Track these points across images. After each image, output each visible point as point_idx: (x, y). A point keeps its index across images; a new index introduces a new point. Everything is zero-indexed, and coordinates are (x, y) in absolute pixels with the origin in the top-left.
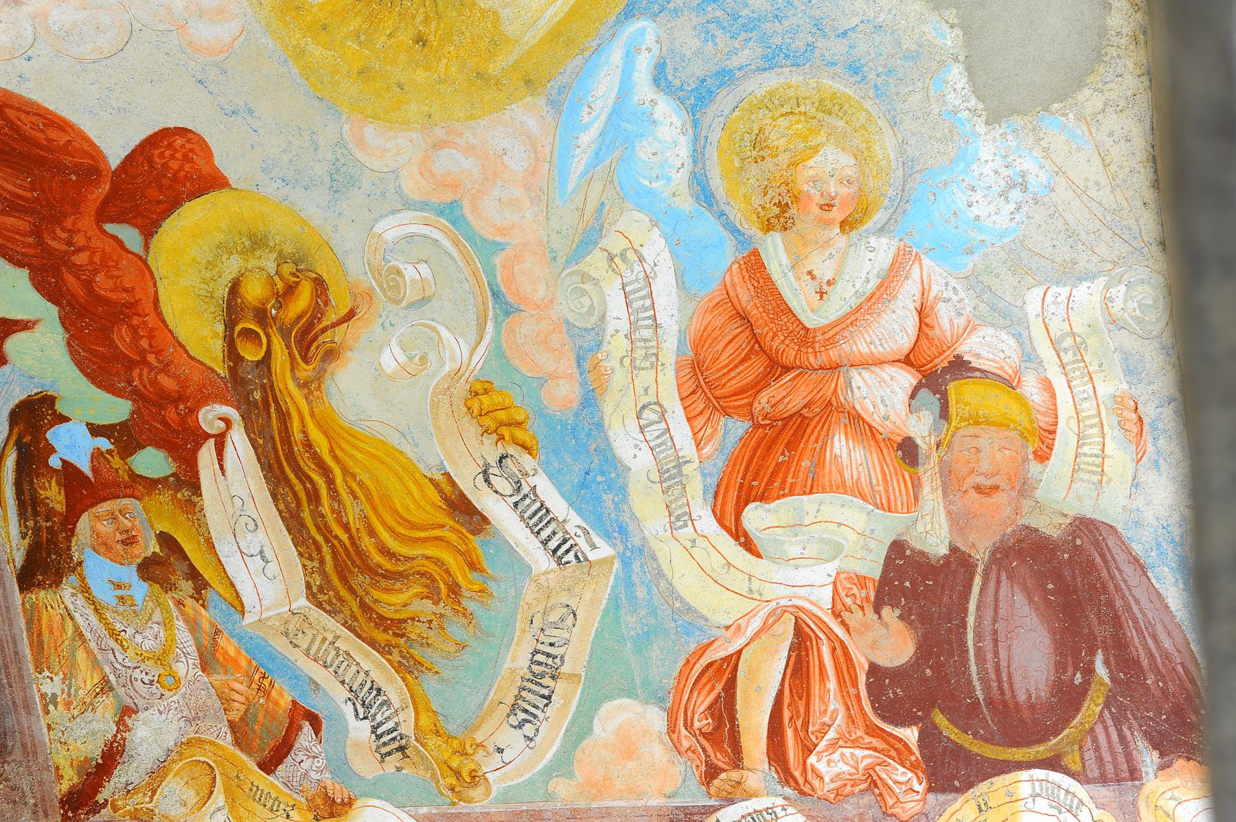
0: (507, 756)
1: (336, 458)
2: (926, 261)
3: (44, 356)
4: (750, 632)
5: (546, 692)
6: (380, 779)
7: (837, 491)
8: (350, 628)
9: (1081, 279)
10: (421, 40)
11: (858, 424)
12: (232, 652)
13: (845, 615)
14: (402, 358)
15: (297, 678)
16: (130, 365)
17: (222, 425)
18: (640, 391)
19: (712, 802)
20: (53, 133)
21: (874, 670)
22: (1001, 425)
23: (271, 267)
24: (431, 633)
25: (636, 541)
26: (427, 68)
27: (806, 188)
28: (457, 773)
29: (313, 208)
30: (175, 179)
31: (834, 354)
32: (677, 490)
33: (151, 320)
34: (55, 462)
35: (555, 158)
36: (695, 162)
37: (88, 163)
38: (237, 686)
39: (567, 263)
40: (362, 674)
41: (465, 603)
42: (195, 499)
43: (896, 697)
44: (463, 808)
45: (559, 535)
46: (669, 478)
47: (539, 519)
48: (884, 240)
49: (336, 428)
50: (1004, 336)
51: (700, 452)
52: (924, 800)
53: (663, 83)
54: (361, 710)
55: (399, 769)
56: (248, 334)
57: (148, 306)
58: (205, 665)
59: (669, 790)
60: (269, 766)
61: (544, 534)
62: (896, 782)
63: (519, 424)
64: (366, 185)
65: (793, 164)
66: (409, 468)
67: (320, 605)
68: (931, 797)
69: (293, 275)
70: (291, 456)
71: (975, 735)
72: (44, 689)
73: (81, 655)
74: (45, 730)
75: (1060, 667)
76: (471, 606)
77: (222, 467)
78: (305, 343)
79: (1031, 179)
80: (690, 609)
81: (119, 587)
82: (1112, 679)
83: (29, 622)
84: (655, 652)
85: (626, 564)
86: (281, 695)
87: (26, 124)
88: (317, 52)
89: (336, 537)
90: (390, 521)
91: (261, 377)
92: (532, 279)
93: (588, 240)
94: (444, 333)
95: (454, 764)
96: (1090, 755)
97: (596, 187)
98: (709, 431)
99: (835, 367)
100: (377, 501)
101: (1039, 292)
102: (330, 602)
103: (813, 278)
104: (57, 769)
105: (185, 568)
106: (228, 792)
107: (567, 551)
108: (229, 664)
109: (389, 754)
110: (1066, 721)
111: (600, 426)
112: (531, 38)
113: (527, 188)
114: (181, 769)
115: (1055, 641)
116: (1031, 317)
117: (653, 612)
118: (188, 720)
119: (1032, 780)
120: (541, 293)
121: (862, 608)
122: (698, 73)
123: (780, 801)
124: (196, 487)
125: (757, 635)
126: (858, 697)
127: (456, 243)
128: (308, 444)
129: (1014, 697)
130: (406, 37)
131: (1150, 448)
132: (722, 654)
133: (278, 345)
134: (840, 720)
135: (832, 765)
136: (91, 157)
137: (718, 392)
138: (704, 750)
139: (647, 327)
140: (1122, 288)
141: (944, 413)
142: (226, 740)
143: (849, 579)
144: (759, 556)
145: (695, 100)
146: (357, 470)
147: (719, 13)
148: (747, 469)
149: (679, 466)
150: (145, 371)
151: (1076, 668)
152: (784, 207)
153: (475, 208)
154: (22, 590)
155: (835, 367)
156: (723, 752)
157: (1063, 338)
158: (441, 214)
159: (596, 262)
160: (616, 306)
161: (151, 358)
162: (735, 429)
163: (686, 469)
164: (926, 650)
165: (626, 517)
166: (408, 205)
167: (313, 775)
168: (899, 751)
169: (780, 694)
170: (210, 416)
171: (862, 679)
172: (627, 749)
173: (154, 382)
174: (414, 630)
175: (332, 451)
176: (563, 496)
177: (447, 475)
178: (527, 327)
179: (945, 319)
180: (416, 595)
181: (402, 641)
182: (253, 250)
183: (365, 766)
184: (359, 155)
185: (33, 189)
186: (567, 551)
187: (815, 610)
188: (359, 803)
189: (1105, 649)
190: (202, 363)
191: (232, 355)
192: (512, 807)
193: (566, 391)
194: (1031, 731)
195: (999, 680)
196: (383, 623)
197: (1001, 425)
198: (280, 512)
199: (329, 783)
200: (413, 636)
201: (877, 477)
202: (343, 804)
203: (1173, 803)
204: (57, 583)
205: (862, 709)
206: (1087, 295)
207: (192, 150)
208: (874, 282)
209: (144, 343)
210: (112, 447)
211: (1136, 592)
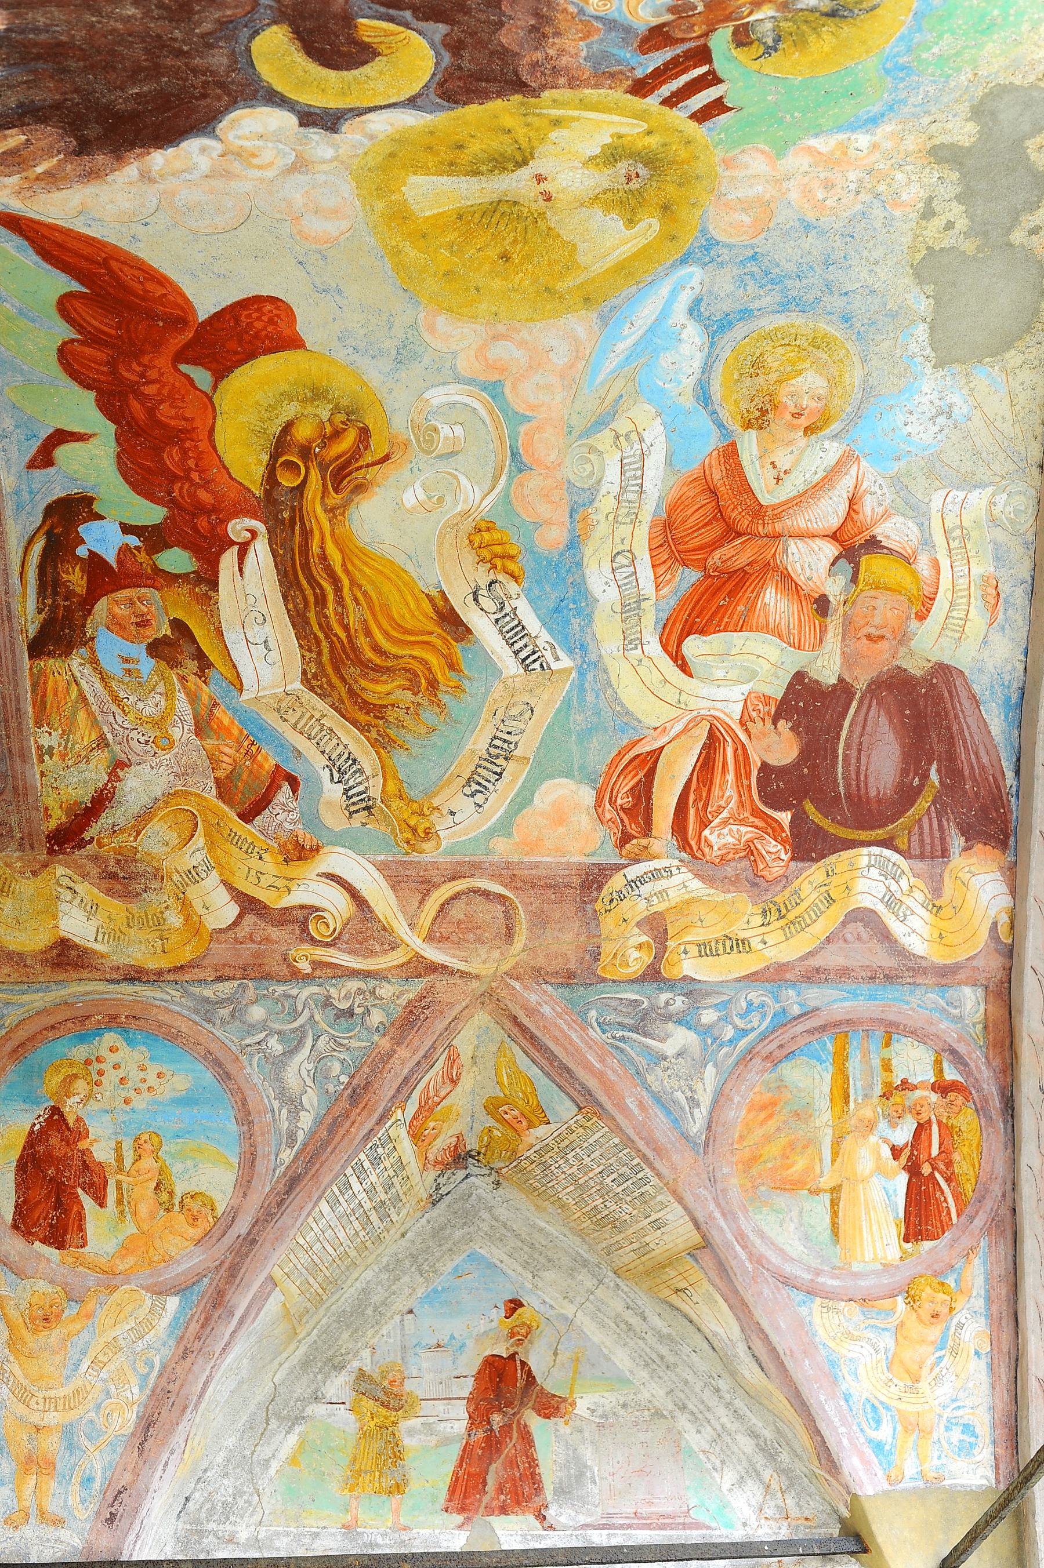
0: (457, 818)
1: (346, 571)
2: (864, 463)
3: (93, 463)
4: (673, 733)
5: (498, 770)
6: (348, 831)
7: (761, 631)
8: (336, 709)
9: (975, 487)
10: (505, 257)
11: (788, 582)
12: (226, 722)
13: (750, 724)
14: (422, 496)
15: (281, 745)
16: (174, 478)
17: (248, 535)
18: (618, 540)
19: (622, 861)
20: (150, 286)
21: (765, 767)
22: (895, 591)
23: (325, 415)
24: (407, 717)
25: (593, 657)
26: (505, 279)
27: (784, 399)
28: (414, 830)
29: (375, 374)
30: (256, 336)
31: (778, 526)
32: (634, 620)
33: (203, 445)
34: (82, 552)
35: (592, 358)
36: (703, 372)
37: (174, 311)
38: (226, 750)
39: (580, 437)
40: (341, 747)
41: (440, 695)
42: (211, 593)
43: (776, 787)
44: (415, 857)
45: (530, 648)
46: (629, 611)
47: (514, 632)
48: (835, 444)
49: (351, 546)
50: (910, 524)
51: (658, 592)
52: (787, 866)
53: (696, 313)
54: (336, 776)
55: (364, 824)
56: (290, 466)
57: (203, 435)
58: (200, 730)
59: (588, 851)
60: (247, 816)
61: (517, 646)
62: (768, 852)
63: (511, 557)
64: (426, 361)
65: (779, 382)
66: (410, 585)
67: (312, 689)
68: (793, 864)
69: (343, 423)
70: (306, 567)
71: (833, 820)
72: (41, 742)
73: (81, 716)
74: (38, 776)
75: (905, 772)
76: (445, 698)
77: (241, 570)
78: (339, 477)
79: (956, 410)
80: (628, 713)
81: (127, 661)
82: (941, 783)
83: (35, 685)
84: (594, 744)
85: (582, 674)
86: (266, 759)
87: (127, 275)
88: (411, 253)
89: (336, 635)
90: (386, 625)
91: (292, 500)
92: (547, 447)
93: (602, 422)
94: (463, 480)
95: (412, 823)
96: (915, 838)
97: (620, 383)
98: (668, 577)
99: (777, 536)
100: (377, 608)
101: (942, 493)
102: (321, 687)
103: (774, 467)
104: (46, 809)
105: (193, 649)
106: (208, 836)
107: (535, 661)
108: (223, 731)
109: (357, 811)
110: (902, 813)
111: (579, 565)
112: (598, 268)
113: (562, 377)
114: (167, 814)
115: (903, 753)
116: (933, 511)
117: (598, 713)
118: (177, 775)
119: (870, 855)
120: (553, 457)
121: (763, 720)
122: (726, 309)
123: (676, 862)
124: (214, 585)
125: (678, 735)
126: (749, 787)
127: (491, 413)
128: (324, 558)
129: (867, 793)
130: (493, 253)
131: (1001, 616)
132: (648, 749)
133: (315, 476)
135: (720, 838)
136: (182, 309)
137: (680, 547)
138: (622, 821)
139: (633, 492)
140: (1005, 496)
141: (854, 579)
142: (211, 793)
143: (758, 698)
144: (691, 676)
145: (716, 328)
146: (364, 582)
147: (755, 269)
148: (693, 608)
149: (639, 602)
150: (187, 485)
151: (916, 774)
152: (764, 412)
153: (514, 387)
154: (31, 657)
155: (777, 536)
156: (638, 824)
157: (954, 529)
158: (485, 389)
159: (605, 438)
160: (612, 473)
161: (195, 476)
162: (691, 576)
163: (643, 605)
164: (806, 755)
165: (588, 638)
166: (458, 380)
167: (287, 826)
168: (774, 829)
169: (690, 780)
170: (238, 527)
171: (755, 773)
172: (559, 817)
173: (193, 495)
174: (392, 715)
175: (344, 564)
176: (538, 617)
177: (442, 592)
178: (533, 482)
179: (869, 507)
180: (399, 687)
181: (381, 722)
182: (313, 400)
183: (334, 820)
184: (426, 336)
185: (119, 327)
186: (535, 661)
187: (727, 720)
188: (325, 850)
189: (939, 761)
190: (241, 484)
191: (271, 479)
192: (457, 858)
193: (556, 535)
194: (870, 818)
195: (858, 780)
196: (366, 707)
197: (895, 591)
198: (288, 611)
199: (300, 834)
200: (391, 719)
201: (794, 622)
202: (311, 850)
203: (969, 875)
204: (67, 653)
205: (751, 796)
206: (978, 499)
207: (278, 316)
208: (821, 474)
209: (191, 463)
210: (140, 544)
211: (969, 720)
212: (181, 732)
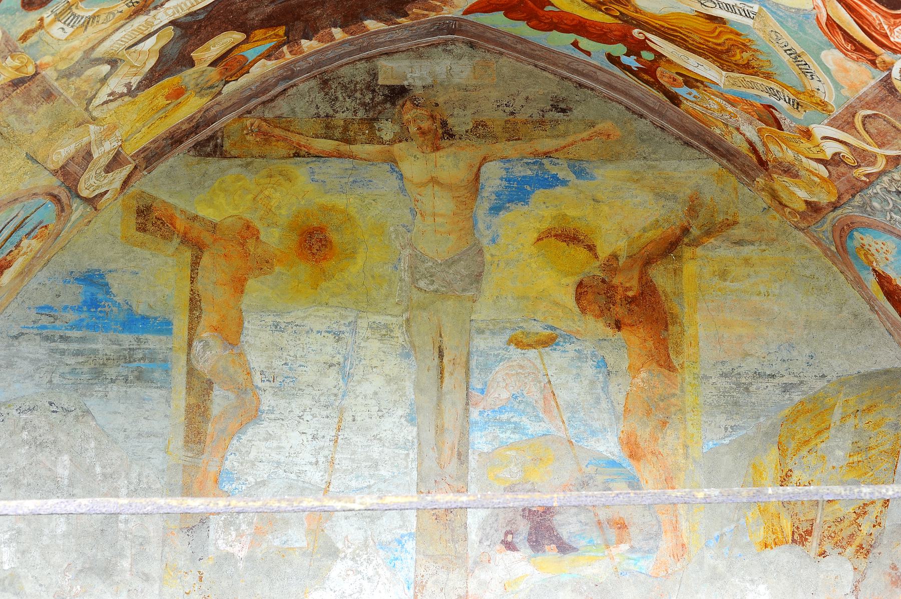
19: (887, 73)
85: (766, 7)
134: (882, 20)
212: (730, 109)
